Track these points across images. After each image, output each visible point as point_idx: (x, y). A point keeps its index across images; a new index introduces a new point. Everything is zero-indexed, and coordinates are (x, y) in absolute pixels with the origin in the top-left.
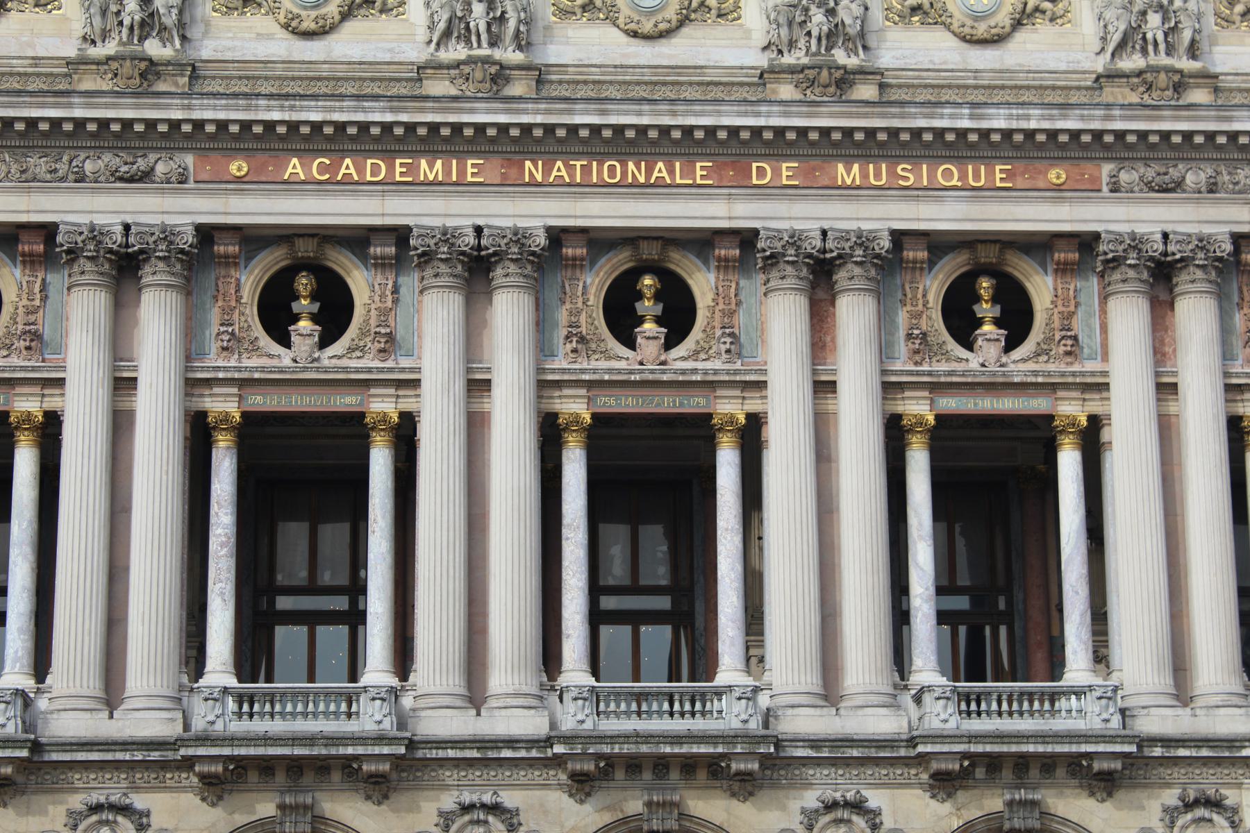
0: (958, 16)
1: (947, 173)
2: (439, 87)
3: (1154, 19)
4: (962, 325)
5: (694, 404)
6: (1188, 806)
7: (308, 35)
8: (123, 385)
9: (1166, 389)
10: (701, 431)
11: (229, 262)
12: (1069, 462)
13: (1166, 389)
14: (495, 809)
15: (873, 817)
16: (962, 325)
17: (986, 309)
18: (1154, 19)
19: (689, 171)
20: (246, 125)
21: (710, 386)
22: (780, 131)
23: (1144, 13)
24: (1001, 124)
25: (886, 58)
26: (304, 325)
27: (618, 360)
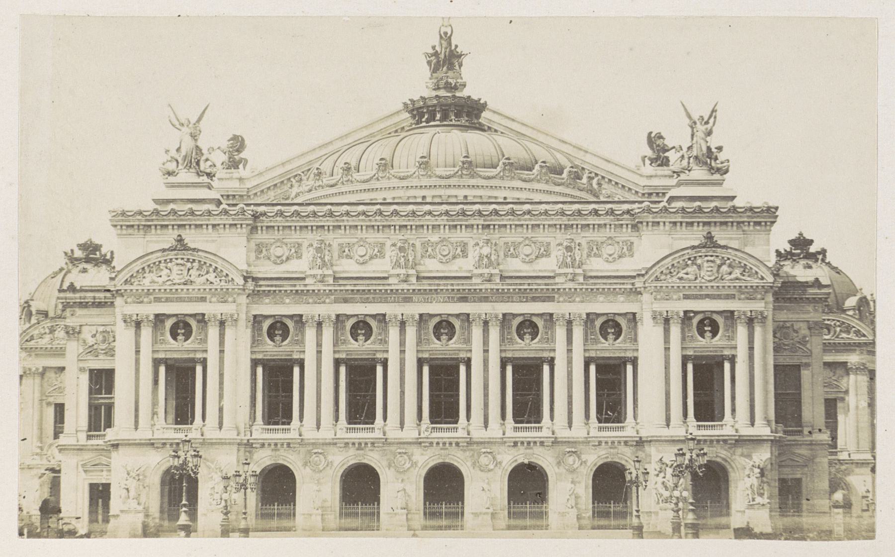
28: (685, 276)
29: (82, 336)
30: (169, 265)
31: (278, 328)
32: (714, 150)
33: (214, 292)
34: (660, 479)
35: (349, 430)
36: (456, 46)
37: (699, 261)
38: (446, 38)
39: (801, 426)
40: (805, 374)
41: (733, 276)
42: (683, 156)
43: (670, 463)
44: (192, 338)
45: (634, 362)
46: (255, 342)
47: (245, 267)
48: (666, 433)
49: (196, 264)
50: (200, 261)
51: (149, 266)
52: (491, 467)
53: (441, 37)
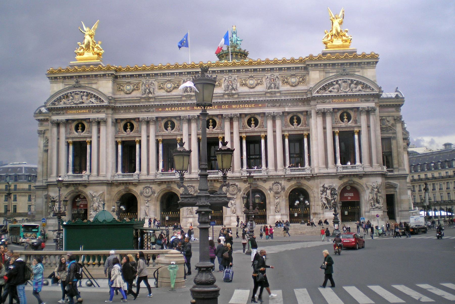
0: (249, 85)
1: (246, 106)
2: (184, 99)
3: (273, 85)
4: (249, 123)
5: (216, 136)
6: (275, 183)
7: (169, 92)
8: (148, 136)
9: (274, 132)
12: (263, 141)
13: (274, 132)
14: (192, 186)
15: (237, 186)
17: (253, 122)
18: (273, 85)
19: (214, 107)
20: (161, 105)
21: (218, 134)
22: (225, 102)
23: (271, 84)
24: (252, 99)
25: (240, 91)
26: (169, 128)
28: (333, 90)
29: (46, 135)
30: (73, 94)
31: (129, 125)
33: (94, 107)
34: (324, 196)
37: (340, 82)
39: (392, 168)
40: (394, 142)
41: (357, 89)
43: (328, 187)
44: (85, 131)
45: (308, 136)
46: (117, 132)
47: (110, 95)
48: (325, 171)
49: (85, 94)
50: (87, 92)
51: (63, 95)
52: (235, 192)
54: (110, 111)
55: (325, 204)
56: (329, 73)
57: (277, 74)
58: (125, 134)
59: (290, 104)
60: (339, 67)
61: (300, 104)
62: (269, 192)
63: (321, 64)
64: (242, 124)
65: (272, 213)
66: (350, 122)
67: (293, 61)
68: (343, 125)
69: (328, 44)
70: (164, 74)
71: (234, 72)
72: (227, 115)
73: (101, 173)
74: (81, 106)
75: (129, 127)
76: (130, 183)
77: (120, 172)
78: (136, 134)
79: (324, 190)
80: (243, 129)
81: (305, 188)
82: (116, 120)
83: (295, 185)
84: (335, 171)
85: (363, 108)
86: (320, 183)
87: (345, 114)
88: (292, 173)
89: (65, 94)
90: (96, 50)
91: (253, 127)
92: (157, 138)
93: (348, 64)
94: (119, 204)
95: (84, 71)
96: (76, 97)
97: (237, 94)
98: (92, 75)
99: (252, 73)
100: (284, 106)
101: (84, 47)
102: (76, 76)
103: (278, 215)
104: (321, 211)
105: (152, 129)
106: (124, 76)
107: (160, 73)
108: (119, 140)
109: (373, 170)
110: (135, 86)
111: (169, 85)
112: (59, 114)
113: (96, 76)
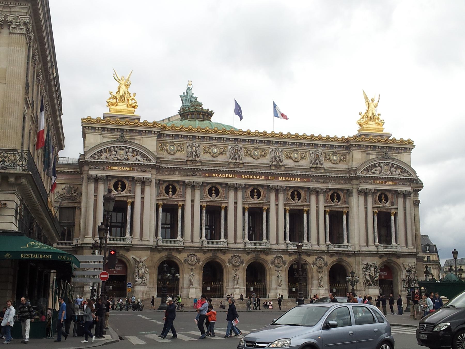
1: (292, 179)
2: (232, 166)
6: (318, 258)
7: (215, 157)
8: (193, 201)
9: (317, 207)
10: (261, 210)
11: (205, 186)
12: (305, 215)
13: (317, 207)
14: (238, 256)
15: (282, 258)
16: (293, 198)
17: (296, 196)
18: (318, 160)
27: (252, 201)
28: (375, 172)
30: (116, 149)
31: (170, 187)
32: (377, 115)
33: (139, 166)
34: (367, 273)
35: (209, 243)
36: (193, 94)
37: (382, 165)
38: (189, 89)
41: (397, 173)
42: (363, 118)
44: (126, 190)
46: (159, 194)
47: (156, 154)
49: (131, 150)
50: (132, 149)
51: (104, 149)
52: (280, 265)
53: (187, 89)
54: (154, 171)
55: (368, 281)
56: (370, 154)
57: (320, 150)
58: (166, 197)
59: (333, 181)
60: (379, 150)
61: (342, 182)
62: (312, 266)
63: (363, 145)
64: (286, 197)
65: (315, 287)
66: (387, 203)
67: (336, 139)
68: (381, 205)
69: (365, 126)
70: (211, 138)
71: (281, 144)
72: (274, 187)
73: (144, 237)
74: (126, 163)
75: (171, 190)
76: (174, 249)
77: (160, 237)
78: (179, 198)
79: (367, 267)
80: (287, 201)
81: (344, 264)
82: (159, 180)
83: (337, 261)
84: (375, 249)
85: (401, 191)
86: (362, 260)
87: (383, 196)
88: (336, 249)
89: (107, 148)
90: (130, 102)
91: (297, 201)
92: (202, 204)
93: (388, 148)
94: (173, 272)
95: (127, 125)
96: (122, 152)
97: (284, 166)
98: (136, 130)
99: (297, 146)
100: (327, 183)
101: (118, 98)
102: (117, 129)
103: (323, 290)
104: (363, 288)
105: (198, 194)
106: (169, 135)
107: (207, 137)
108: (161, 203)
109: (409, 251)
110: (180, 147)
111: (215, 150)
112: (99, 168)
113: (140, 131)
